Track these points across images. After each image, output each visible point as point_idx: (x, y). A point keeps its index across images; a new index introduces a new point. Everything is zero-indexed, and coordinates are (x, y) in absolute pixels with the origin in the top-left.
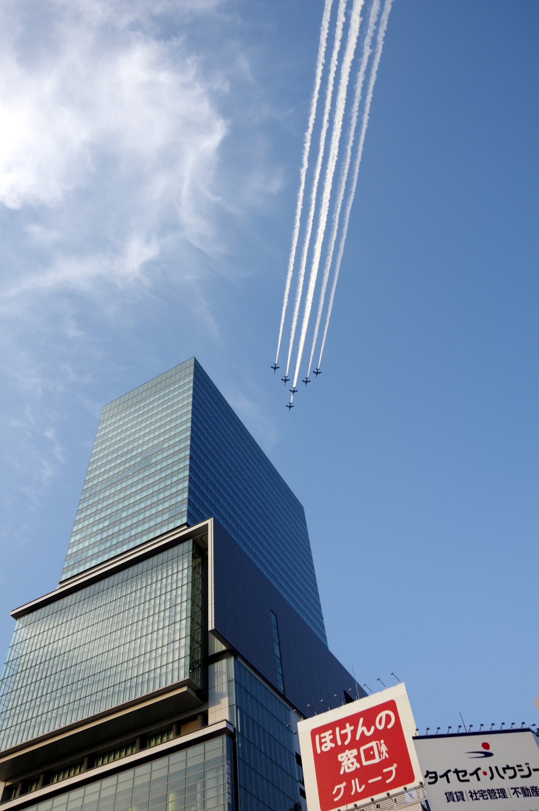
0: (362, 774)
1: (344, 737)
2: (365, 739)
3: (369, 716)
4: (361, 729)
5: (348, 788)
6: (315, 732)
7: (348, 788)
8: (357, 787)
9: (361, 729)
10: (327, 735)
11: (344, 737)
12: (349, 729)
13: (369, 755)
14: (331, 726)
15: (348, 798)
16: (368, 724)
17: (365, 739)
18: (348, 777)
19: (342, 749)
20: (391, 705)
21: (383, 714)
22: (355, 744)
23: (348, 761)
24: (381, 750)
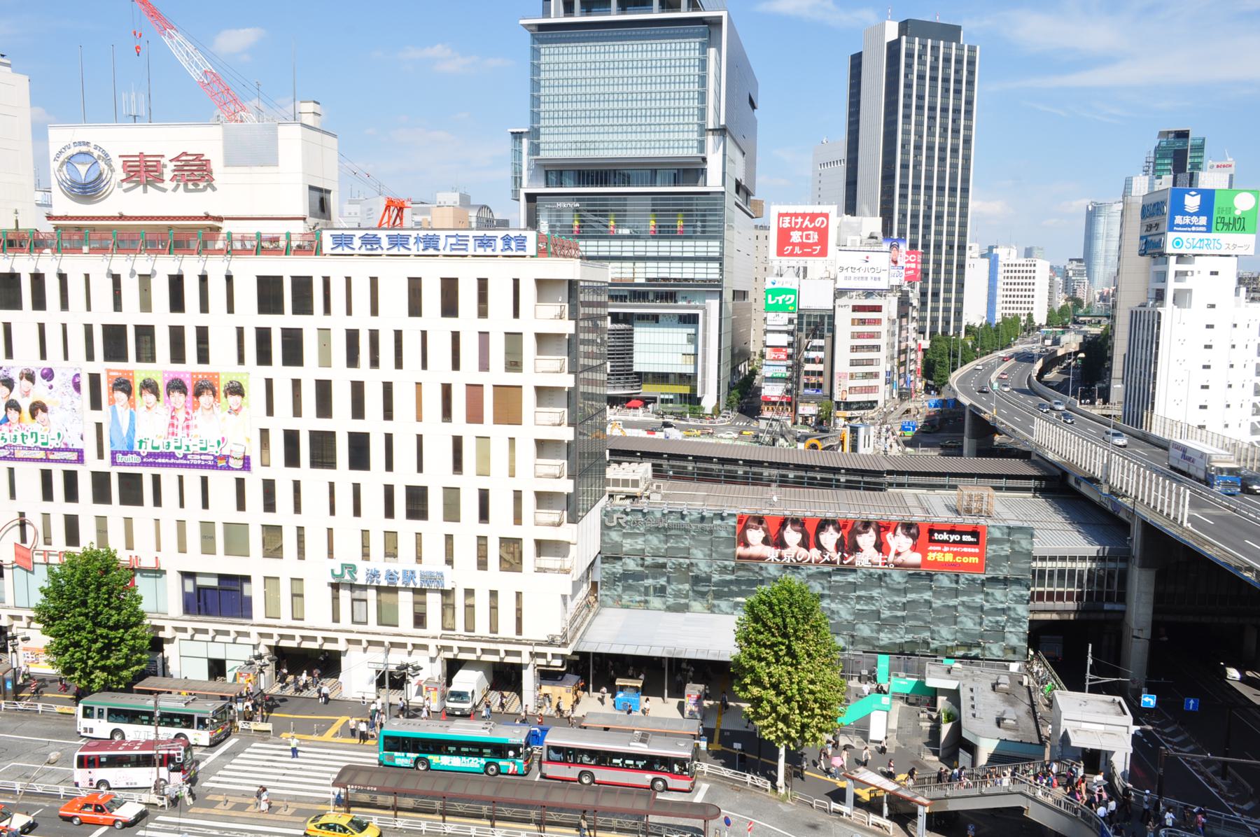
0: (802, 245)
1: (796, 223)
2: (807, 229)
3: (813, 217)
4: (807, 222)
5: (793, 250)
6: (780, 215)
7: (793, 250)
8: (797, 250)
9: (807, 222)
10: (787, 219)
11: (796, 223)
12: (800, 220)
13: (808, 237)
14: (790, 215)
15: (792, 254)
16: (812, 221)
17: (807, 229)
18: (794, 244)
19: (795, 229)
20: (826, 216)
21: (820, 219)
22: (800, 229)
23: (796, 237)
24: (814, 237)
